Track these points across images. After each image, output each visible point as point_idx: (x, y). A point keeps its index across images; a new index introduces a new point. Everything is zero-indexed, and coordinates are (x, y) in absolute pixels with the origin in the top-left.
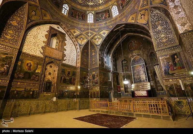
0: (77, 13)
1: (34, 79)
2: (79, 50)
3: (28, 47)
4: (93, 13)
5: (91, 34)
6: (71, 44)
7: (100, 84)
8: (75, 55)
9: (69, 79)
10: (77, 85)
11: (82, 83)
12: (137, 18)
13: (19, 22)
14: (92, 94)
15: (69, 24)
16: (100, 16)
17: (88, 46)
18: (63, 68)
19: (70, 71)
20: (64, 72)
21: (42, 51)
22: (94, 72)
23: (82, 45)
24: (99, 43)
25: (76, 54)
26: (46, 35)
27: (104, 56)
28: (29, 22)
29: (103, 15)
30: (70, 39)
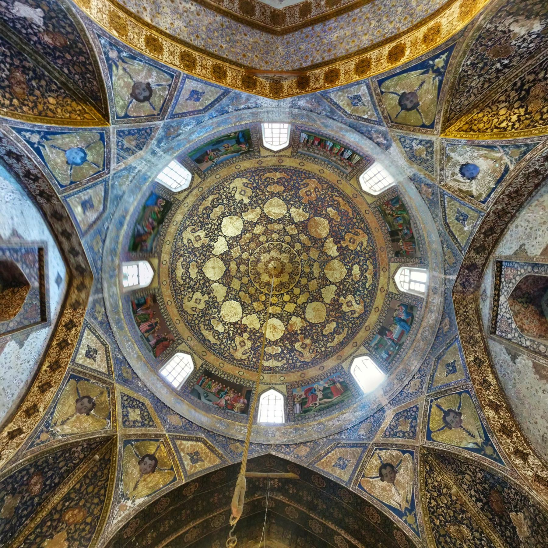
0: (154, 316)
4: (197, 362)
5: (139, 419)
12: (363, 467)
16: (213, 390)
29: (227, 393)
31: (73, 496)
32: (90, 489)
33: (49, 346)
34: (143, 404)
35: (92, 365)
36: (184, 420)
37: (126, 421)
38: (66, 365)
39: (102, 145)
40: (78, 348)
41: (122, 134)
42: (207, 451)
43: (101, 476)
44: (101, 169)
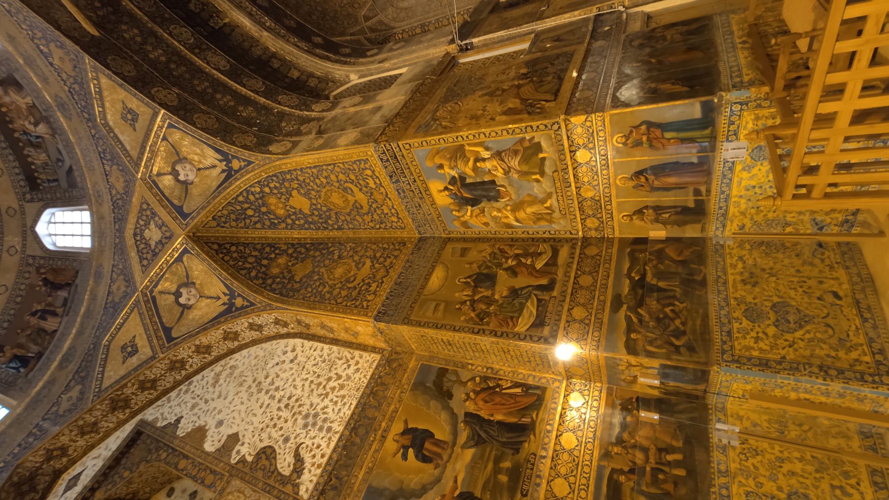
2: (265, 318)
5: (152, 226)
7: (543, 113)
8: (299, 349)
10: (546, 363)
11: (522, 307)
14: (658, 209)
15: (68, 388)
17: (246, 245)
19: (398, 428)
22: (435, 186)
23: (232, 295)
24: (211, 157)
25: (298, 341)
27: (319, 119)
30: (183, 387)
31: (267, 223)
32: (250, 212)
33: (166, 392)
34: (135, 235)
35: (140, 335)
36: (108, 168)
37: (166, 238)
38: (163, 359)
40: (134, 370)
42: (107, 105)
43: (233, 212)
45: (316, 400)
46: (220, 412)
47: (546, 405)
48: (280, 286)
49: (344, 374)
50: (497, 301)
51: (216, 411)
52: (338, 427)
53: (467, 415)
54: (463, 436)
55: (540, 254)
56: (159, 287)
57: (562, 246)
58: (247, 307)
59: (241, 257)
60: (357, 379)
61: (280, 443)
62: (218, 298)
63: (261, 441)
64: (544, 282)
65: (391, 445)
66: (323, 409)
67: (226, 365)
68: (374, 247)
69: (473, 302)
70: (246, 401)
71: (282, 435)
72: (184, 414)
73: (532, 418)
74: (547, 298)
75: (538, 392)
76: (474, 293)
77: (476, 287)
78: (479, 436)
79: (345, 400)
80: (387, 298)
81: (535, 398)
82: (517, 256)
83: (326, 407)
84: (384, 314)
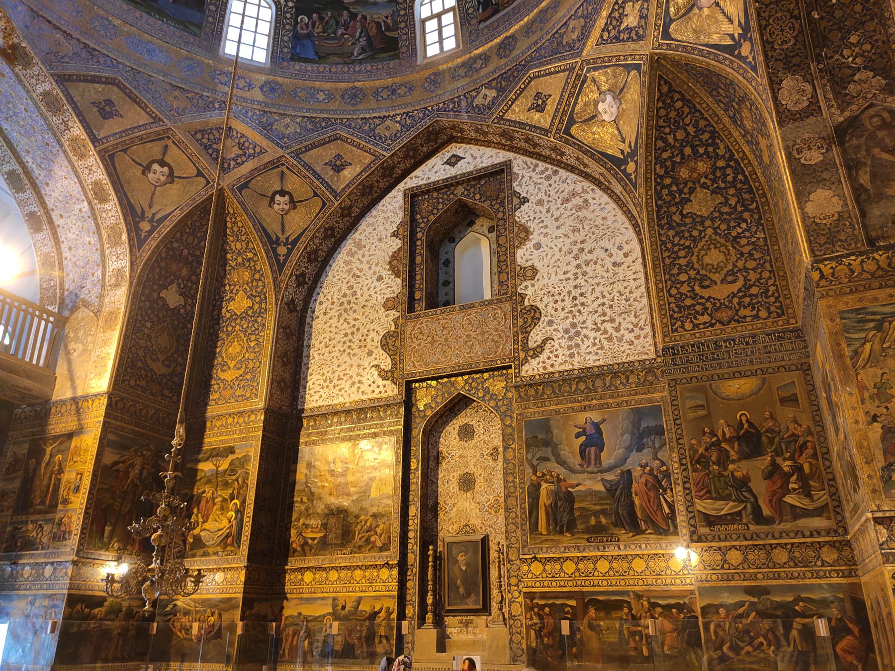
1: (368, 541)
3: (323, 375)
6: (577, 201)
9: (600, 487)
11: (727, 498)
13: (251, 290)
15: (488, 85)
17: (694, 110)
18: (534, 412)
19: (595, 416)
20: (547, 443)
21: (386, 363)
23: (633, 154)
26: (394, 257)
28: (282, 258)
39: (253, 181)
40: (530, 126)
41: (226, 166)
44: (284, 168)
45: (589, 324)
46: (546, 235)
47: (661, 539)
48: (668, 198)
49: (622, 332)
50: (726, 469)
51: (544, 231)
52: (577, 363)
53: (629, 472)
54: (610, 477)
55: (809, 495)
56: (596, 73)
57: (829, 518)
58: (630, 180)
59: (675, 121)
60: (622, 349)
61: (547, 319)
62: (624, 142)
63: (541, 300)
64: (766, 512)
65: (582, 418)
66: (585, 336)
67: (584, 191)
68: (766, 274)
69: (717, 444)
70: (563, 253)
71: (552, 316)
72: (532, 199)
73: (646, 530)
74: (745, 521)
75: (672, 529)
76: (730, 441)
77: (739, 438)
78: (616, 490)
79: (600, 352)
80: (693, 346)
81: (665, 528)
82: (798, 469)
83: (588, 338)
84: (674, 354)
